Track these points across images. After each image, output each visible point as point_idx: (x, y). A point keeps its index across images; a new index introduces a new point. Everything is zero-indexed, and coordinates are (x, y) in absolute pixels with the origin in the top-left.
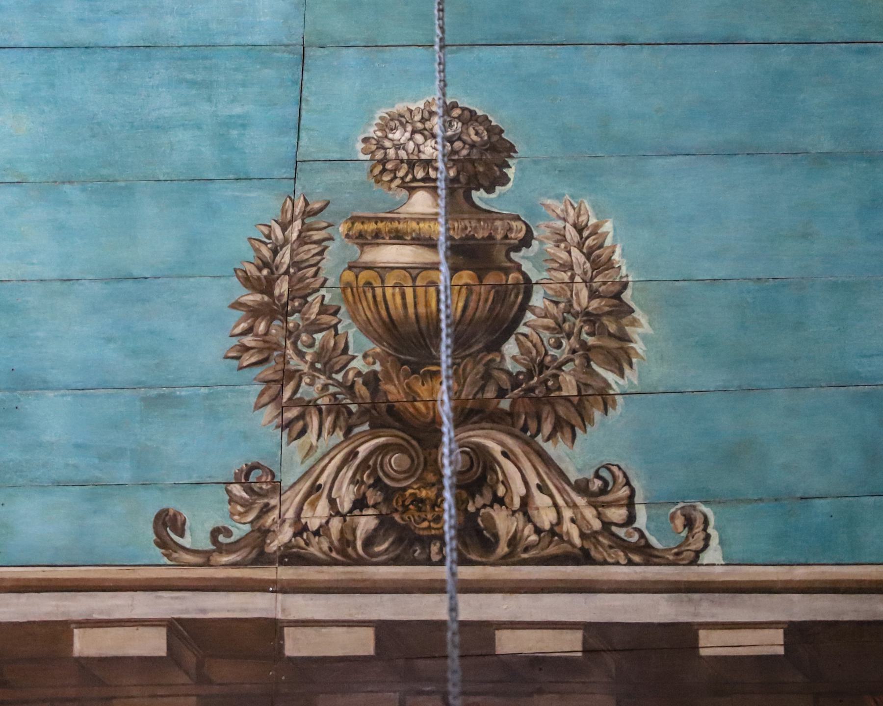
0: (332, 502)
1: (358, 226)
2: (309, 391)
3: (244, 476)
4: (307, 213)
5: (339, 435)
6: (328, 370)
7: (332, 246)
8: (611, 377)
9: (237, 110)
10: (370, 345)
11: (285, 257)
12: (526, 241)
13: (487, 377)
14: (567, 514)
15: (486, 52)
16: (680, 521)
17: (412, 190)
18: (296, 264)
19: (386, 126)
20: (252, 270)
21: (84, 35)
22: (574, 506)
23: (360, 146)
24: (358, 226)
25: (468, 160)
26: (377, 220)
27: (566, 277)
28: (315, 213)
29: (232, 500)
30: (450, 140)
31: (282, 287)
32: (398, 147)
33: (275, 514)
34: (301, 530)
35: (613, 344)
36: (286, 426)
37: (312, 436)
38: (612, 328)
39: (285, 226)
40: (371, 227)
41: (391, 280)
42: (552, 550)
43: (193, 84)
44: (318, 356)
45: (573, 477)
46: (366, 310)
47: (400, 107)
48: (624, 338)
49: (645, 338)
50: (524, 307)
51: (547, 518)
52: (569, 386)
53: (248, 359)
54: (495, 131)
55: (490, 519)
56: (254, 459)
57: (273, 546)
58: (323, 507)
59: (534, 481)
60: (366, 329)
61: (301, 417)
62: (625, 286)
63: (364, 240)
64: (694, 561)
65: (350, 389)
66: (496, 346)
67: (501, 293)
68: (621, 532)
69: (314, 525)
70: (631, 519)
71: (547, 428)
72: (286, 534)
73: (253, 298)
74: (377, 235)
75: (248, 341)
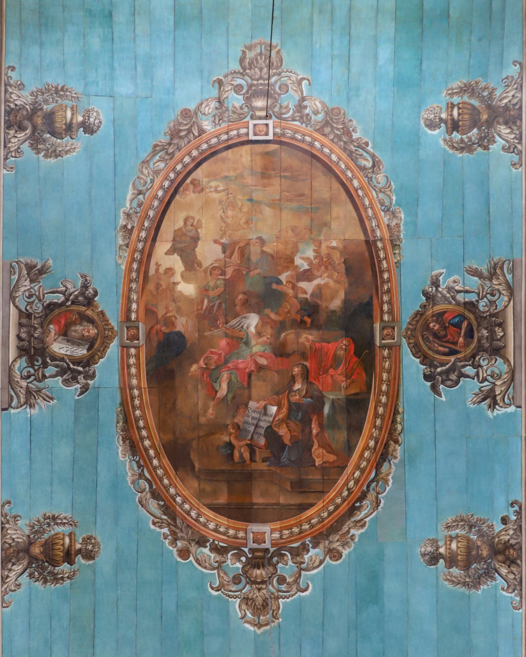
0: (16, 100)
1: (75, 107)
2: (40, 98)
3: (22, 84)
4: (78, 98)
5: (30, 102)
6: (44, 101)
7: (71, 102)
8: (42, 154)
9: (100, 85)
10: (49, 109)
11: (68, 93)
12: (72, 138)
13: (42, 131)
14: (13, 145)
15: (112, 130)
16: (12, 166)
17: (83, 117)
18: (67, 96)
19: (97, 112)
20: (66, 87)
21: (116, 57)
22: (15, 146)
23: (93, 107)
24: (75, 107)
25: (90, 127)
26: (76, 110)
27: (64, 146)
28: (78, 99)
29: (17, 81)
30: (94, 123)
31: (62, 93)
32: (92, 114)
33: (14, 89)
34: (11, 93)
35: (49, 155)
36: (32, 92)
37: (30, 97)
38: (53, 155)
39: (75, 94)
40: (75, 109)
41: (63, 113)
42: (7, 141)
43: (106, 77)
44: (47, 99)
45: (21, 146)
46: (57, 108)
47: (101, 114)
48: (50, 157)
49: (50, 161)
50: (57, 138)
51: (13, 140)
52: (39, 146)
53: (47, 87)
54: (96, 132)
55: (12, 130)
56: (26, 86)
57: (8, 88)
58: (15, 98)
59: (20, 139)
60: (53, 108)
61: (34, 96)
62: (62, 157)
63: (72, 108)
64: (4, 168)
65: (40, 105)
66: (49, 133)
67: (61, 134)
68: (10, 154)
69: (12, 96)
70: (12, 157)
71: (31, 142)
72: (10, 90)
73: (60, 88)
74: (73, 110)
75: (50, 87)
